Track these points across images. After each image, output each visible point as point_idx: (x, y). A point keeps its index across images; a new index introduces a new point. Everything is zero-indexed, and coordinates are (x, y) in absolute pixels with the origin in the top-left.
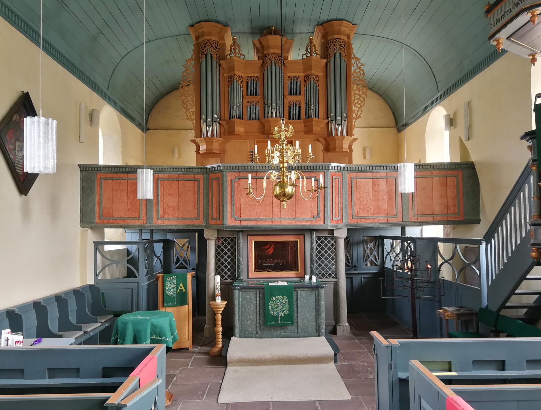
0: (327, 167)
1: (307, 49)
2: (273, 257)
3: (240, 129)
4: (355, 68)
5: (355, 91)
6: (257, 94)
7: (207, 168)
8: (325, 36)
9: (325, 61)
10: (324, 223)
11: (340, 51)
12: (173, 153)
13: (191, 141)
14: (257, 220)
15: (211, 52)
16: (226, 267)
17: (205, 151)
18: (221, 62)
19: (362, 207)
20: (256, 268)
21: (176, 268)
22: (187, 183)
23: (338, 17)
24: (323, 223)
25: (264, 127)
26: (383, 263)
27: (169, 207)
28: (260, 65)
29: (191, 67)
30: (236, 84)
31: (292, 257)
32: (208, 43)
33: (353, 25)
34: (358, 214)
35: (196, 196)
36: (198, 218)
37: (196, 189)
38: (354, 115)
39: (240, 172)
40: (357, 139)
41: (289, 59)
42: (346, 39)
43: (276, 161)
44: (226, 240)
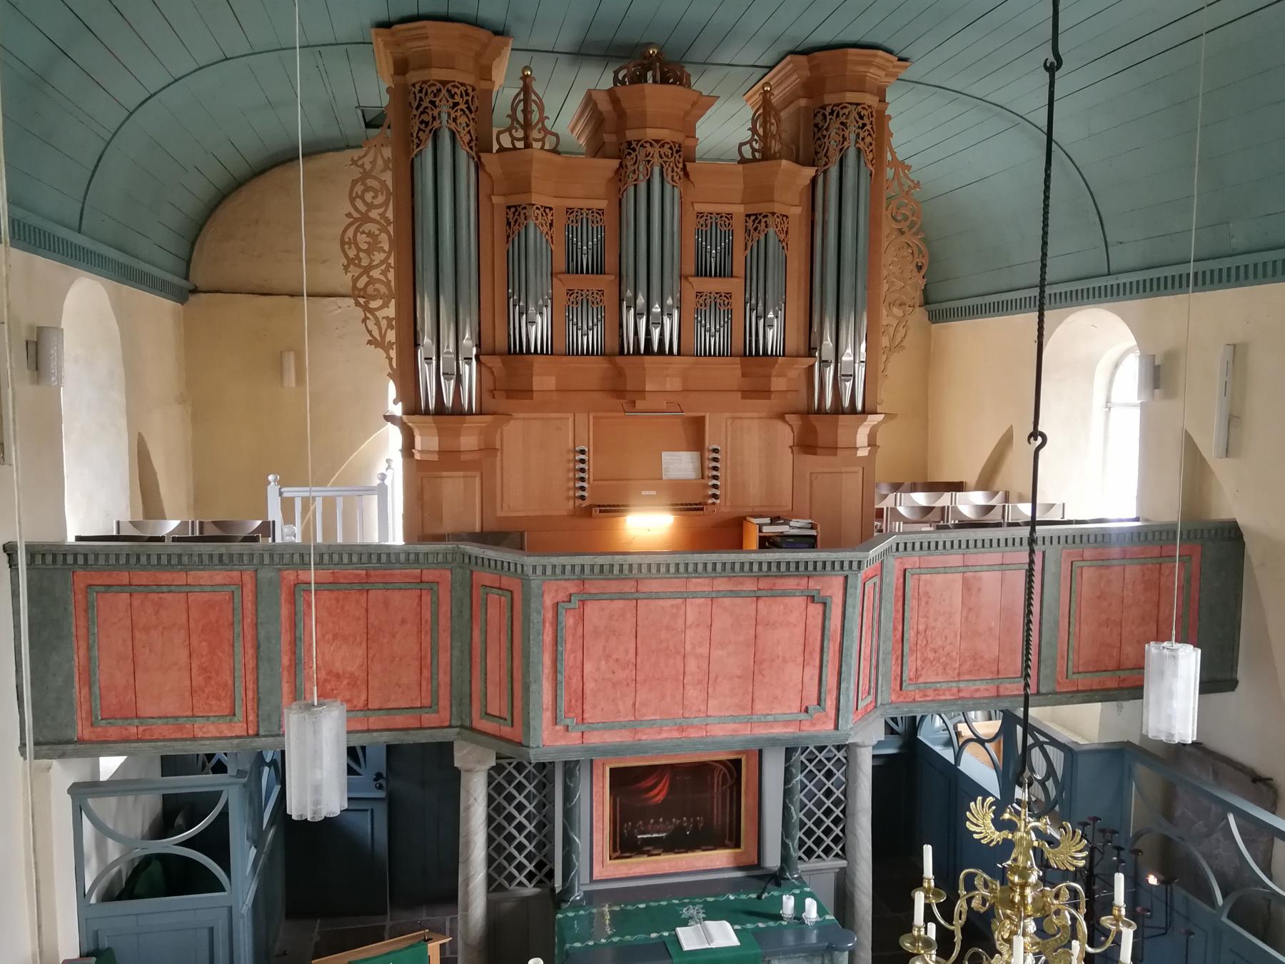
2: (664, 810)
6: (598, 269)
9: (810, 172)
10: (836, 727)
14: (634, 726)
15: (453, 126)
16: (520, 848)
17: (435, 458)
19: (931, 655)
22: (397, 598)
24: (832, 726)
27: (338, 676)
28: (610, 174)
30: (535, 232)
31: (723, 813)
32: (444, 91)
34: (917, 677)
35: (426, 640)
37: (427, 614)
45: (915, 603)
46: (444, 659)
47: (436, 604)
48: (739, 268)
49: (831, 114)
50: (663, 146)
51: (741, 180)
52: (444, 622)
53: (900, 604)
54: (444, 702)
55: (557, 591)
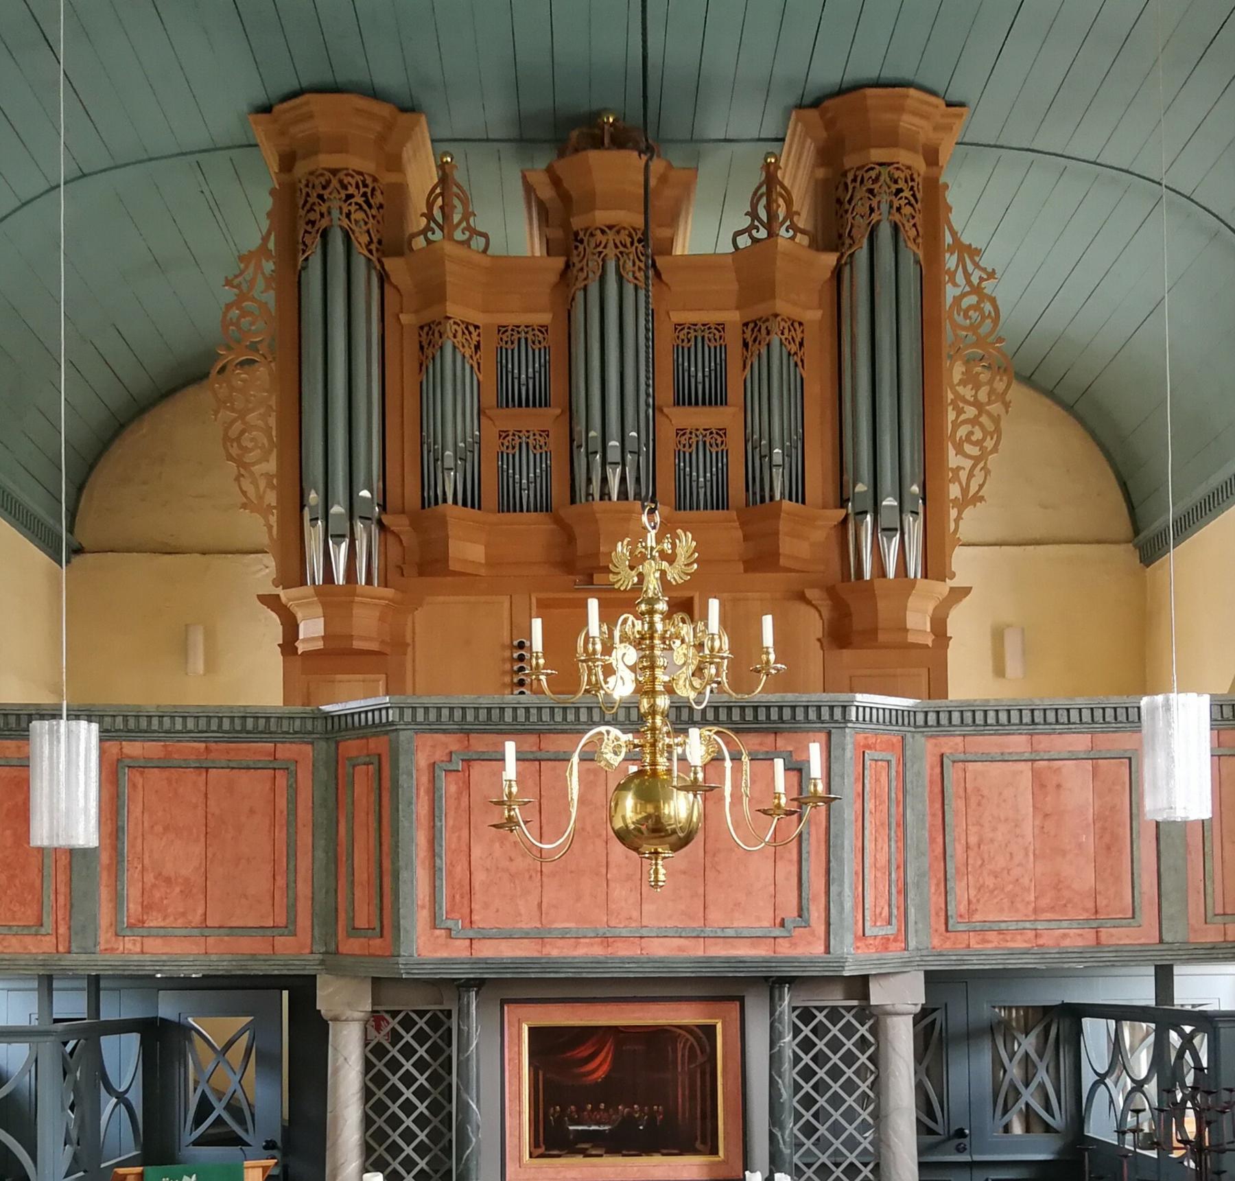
0: (838, 713)
1: (754, 206)
2: (608, 1092)
3: (467, 549)
4: (957, 292)
5: (960, 389)
6: (542, 401)
7: (327, 716)
8: (829, 154)
9: (831, 259)
11: (897, 217)
12: (184, 650)
13: (263, 599)
14: (540, 936)
15: (345, 223)
17: (320, 645)
18: (391, 264)
19: (990, 882)
20: (535, 1143)
21: (197, 1143)
22: (244, 780)
23: (889, 74)
24: (819, 949)
25: (571, 539)
26: (1079, 1118)
27: (168, 880)
28: (553, 278)
29: (260, 283)
31: (693, 1097)
32: (335, 183)
33: (949, 105)
34: (971, 912)
35: (281, 835)
36: (290, 927)
37: (282, 803)
38: (954, 491)
39: (468, 732)
40: (966, 591)
41: (678, 250)
42: (919, 165)
43: (621, 687)
44: (407, 1023)
45: (961, 803)
46: (304, 863)
47: (293, 790)
48: (735, 391)
49: (854, 180)
50: (618, 232)
51: (733, 276)
52: (304, 814)
53: (938, 805)
54: (304, 920)
55: (434, 747)
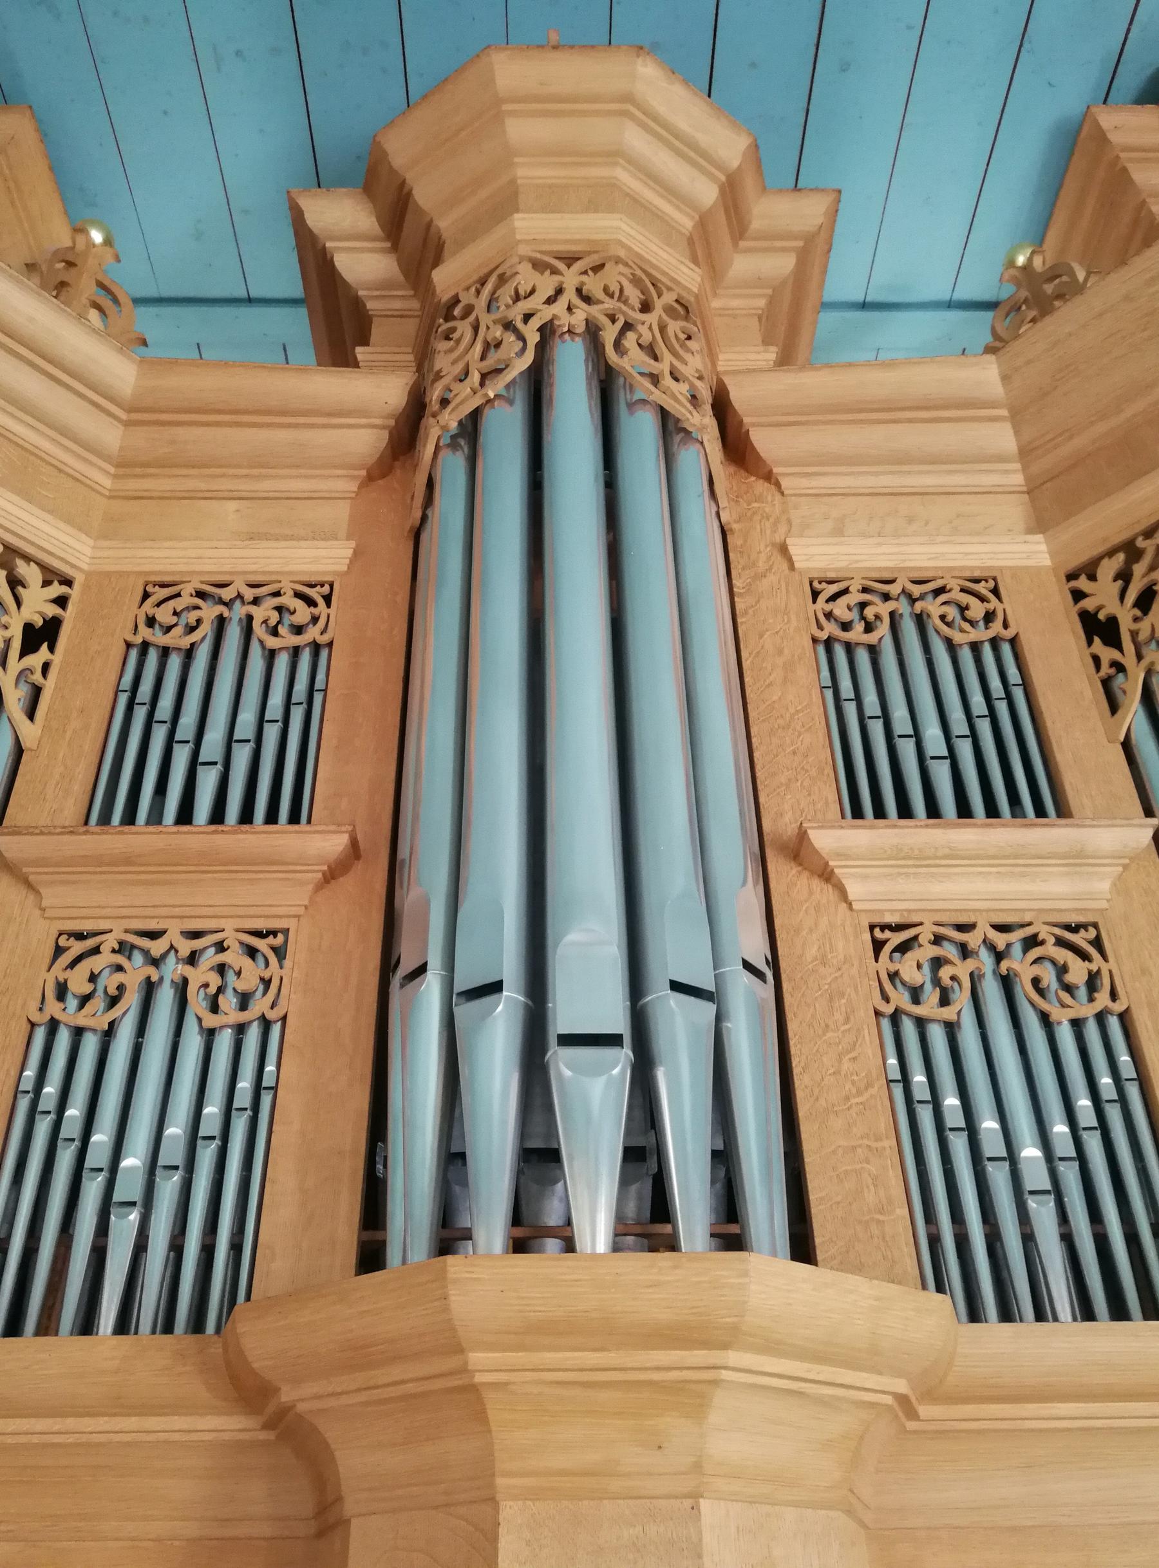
28: (366, 441)
50: (598, 268)
51: (1004, 438)
